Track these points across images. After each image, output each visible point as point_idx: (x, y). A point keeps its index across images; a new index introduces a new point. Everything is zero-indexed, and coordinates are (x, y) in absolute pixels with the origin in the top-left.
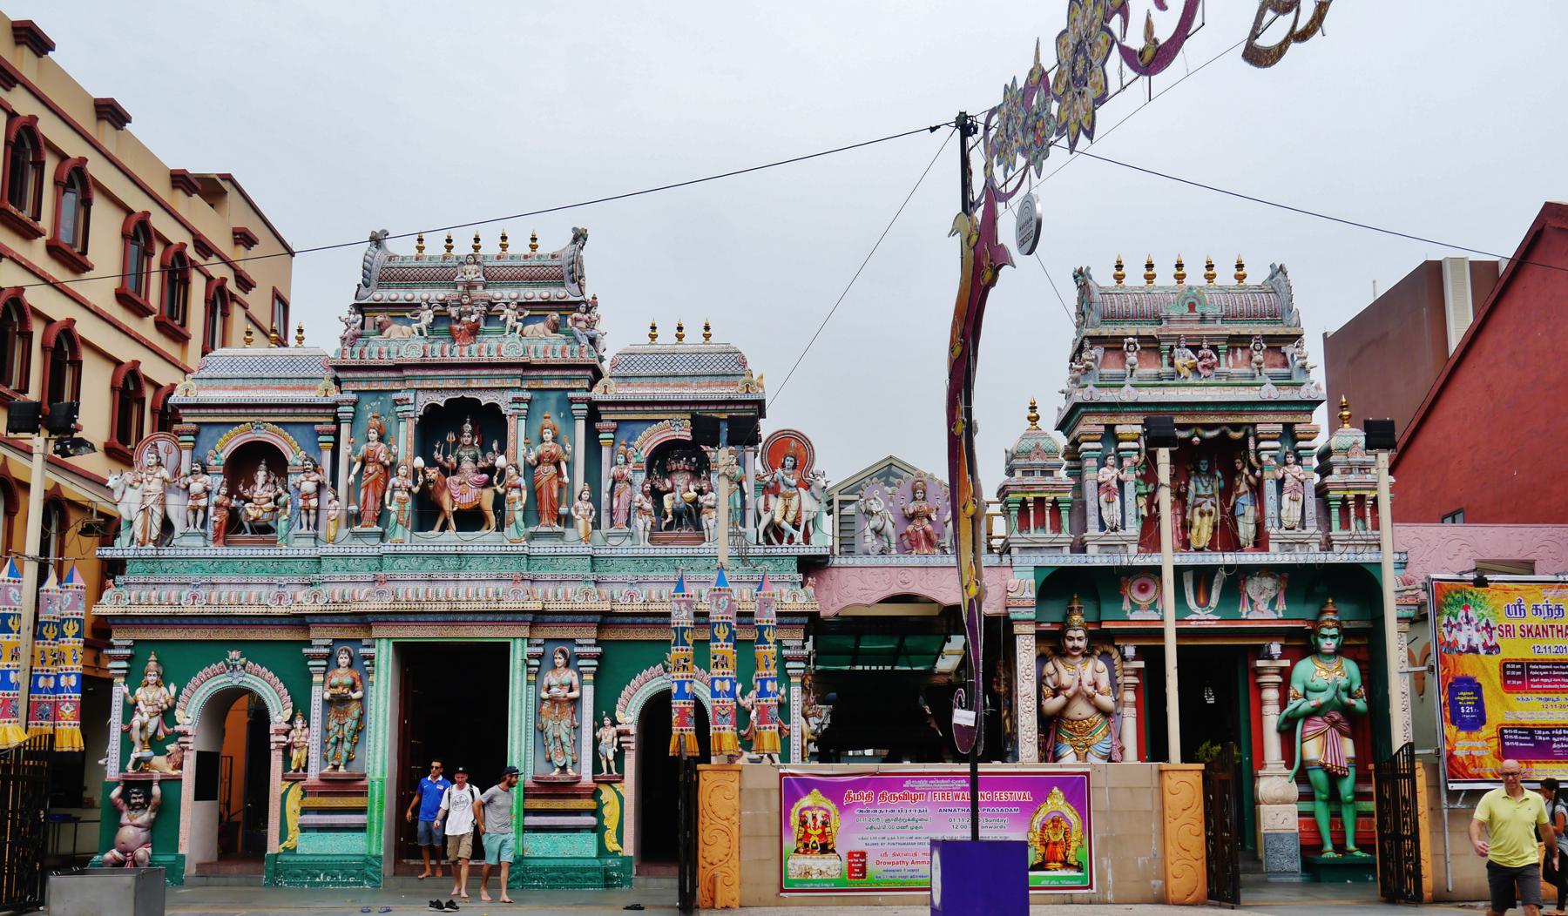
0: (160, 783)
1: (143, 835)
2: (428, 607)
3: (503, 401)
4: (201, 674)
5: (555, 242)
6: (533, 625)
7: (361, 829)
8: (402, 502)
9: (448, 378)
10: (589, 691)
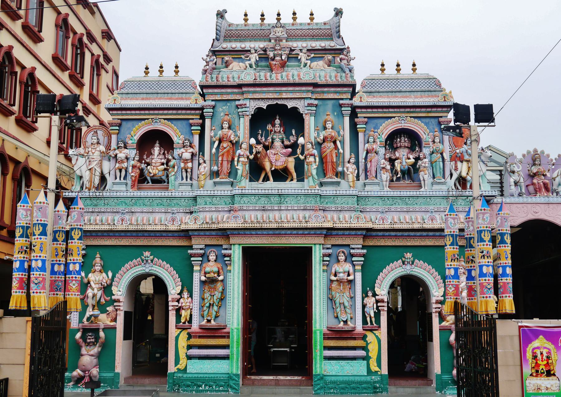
0: (103, 329)
1: (95, 361)
2: (265, 226)
3: (301, 106)
4: (127, 266)
5: (324, 16)
6: (326, 236)
7: (226, 358)
9: (269, 92)
10: (359, 276)
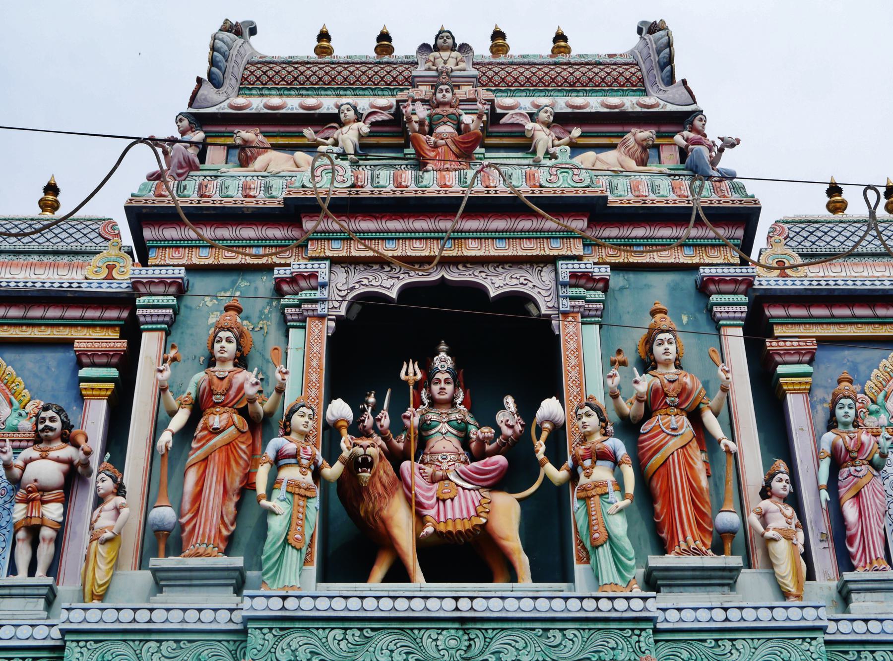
3: (539, 287)
8: (296, 492)
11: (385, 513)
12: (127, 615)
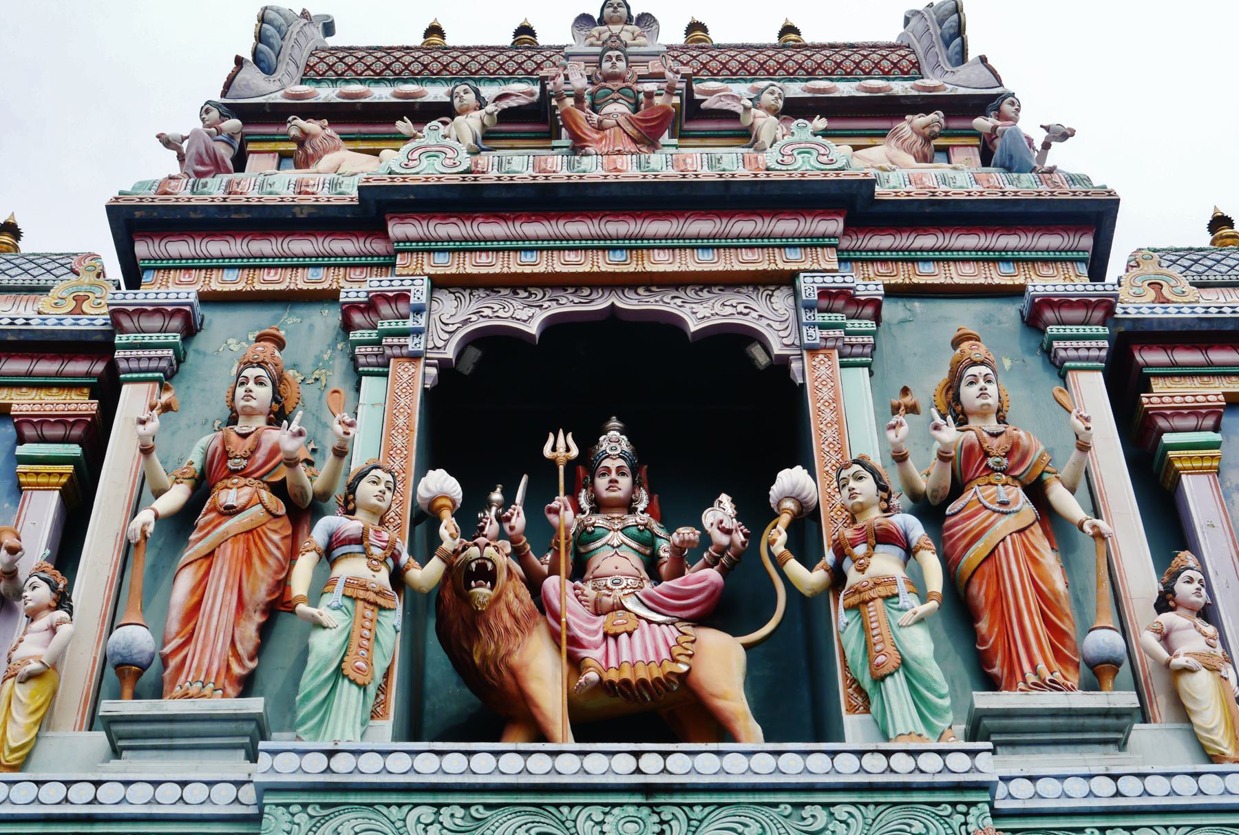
3: (772, 320)
8: (356, 593)
11: (515, 659)
12: (52, 793)
